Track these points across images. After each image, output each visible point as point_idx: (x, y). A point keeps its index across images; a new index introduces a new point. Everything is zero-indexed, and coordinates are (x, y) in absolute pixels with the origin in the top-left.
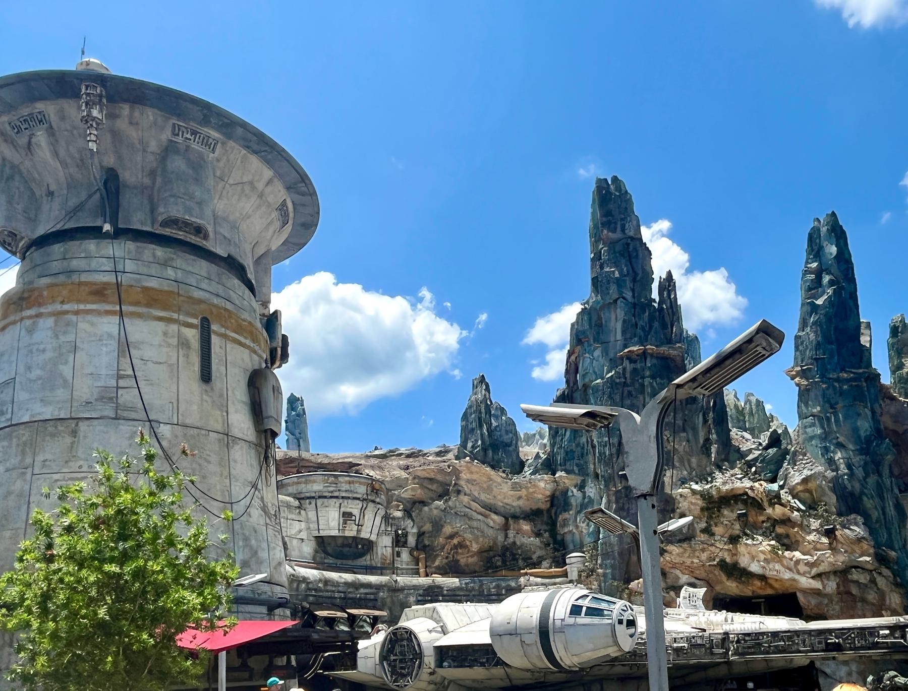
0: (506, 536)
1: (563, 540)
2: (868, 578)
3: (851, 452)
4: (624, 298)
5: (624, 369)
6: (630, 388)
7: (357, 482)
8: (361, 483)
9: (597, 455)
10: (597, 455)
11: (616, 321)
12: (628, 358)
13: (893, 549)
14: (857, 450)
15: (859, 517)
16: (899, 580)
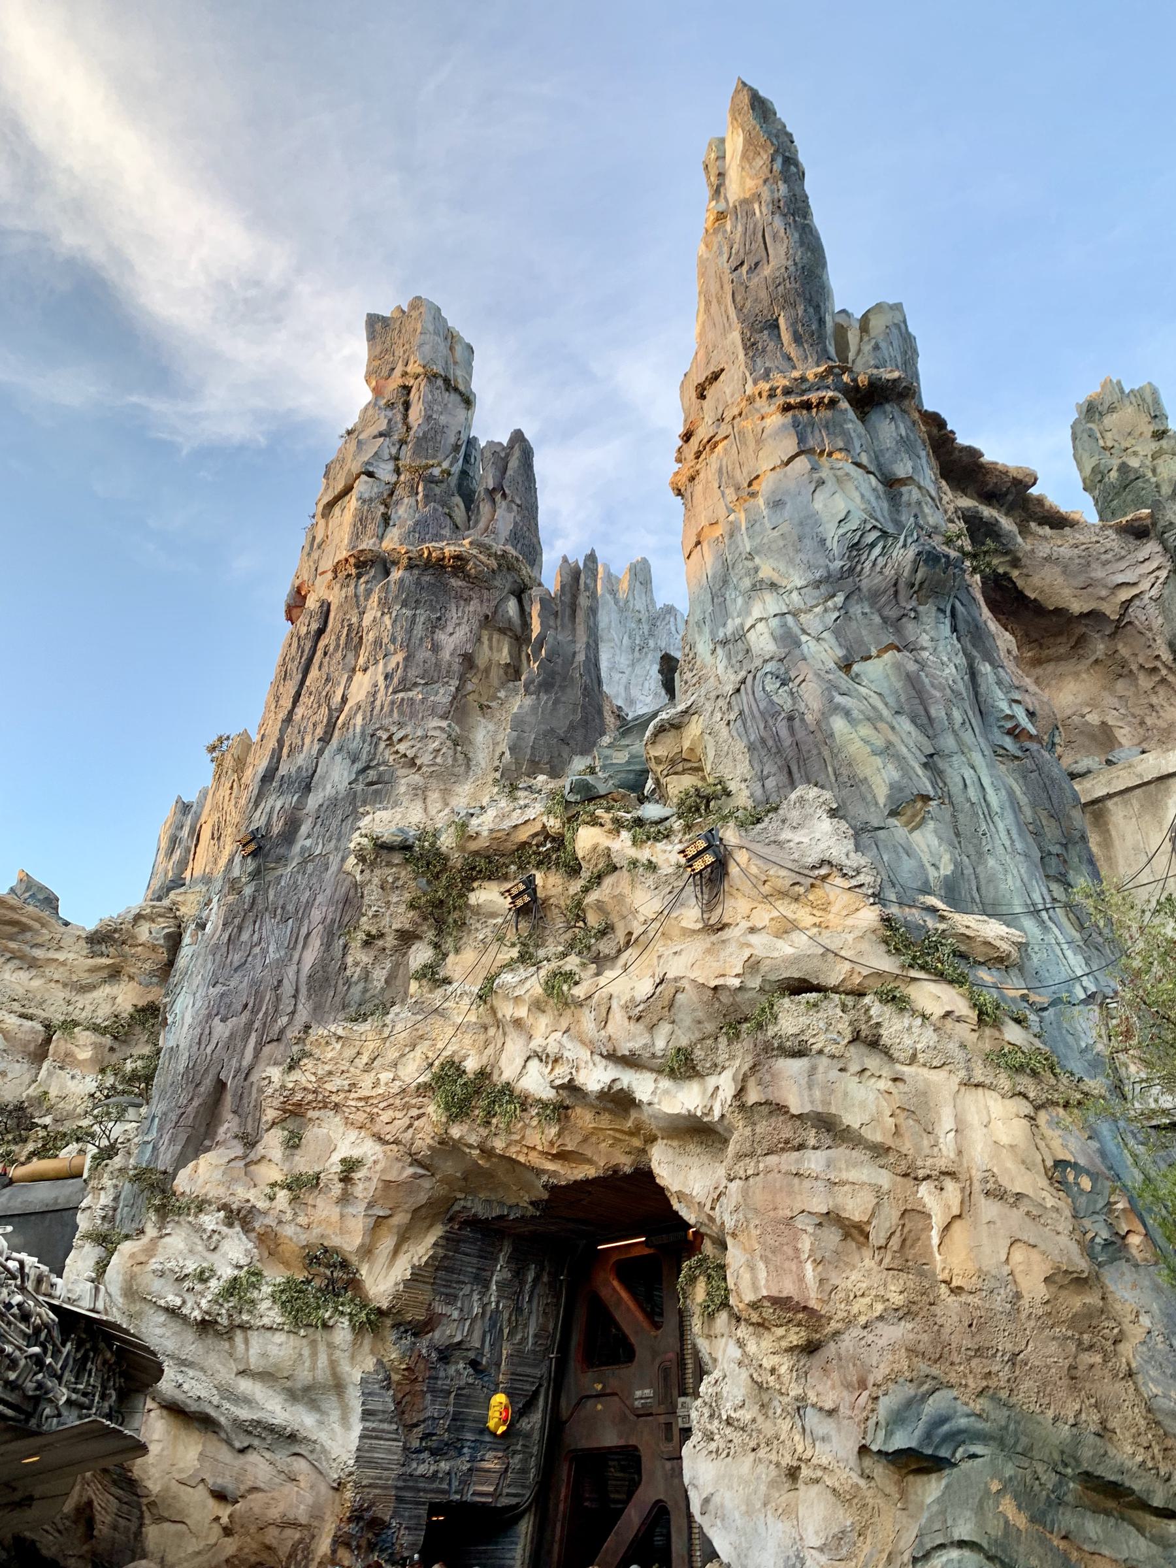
3: (795, 595)
13: (992, 910)
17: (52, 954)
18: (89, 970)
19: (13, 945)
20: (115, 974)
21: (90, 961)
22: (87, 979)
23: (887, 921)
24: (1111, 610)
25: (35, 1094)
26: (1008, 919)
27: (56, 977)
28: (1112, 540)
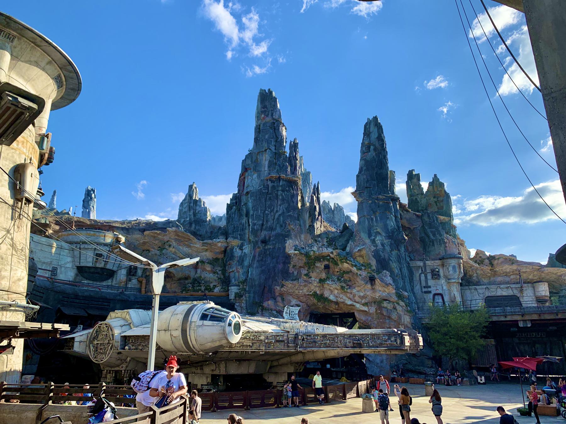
0: (196, 272)
1: (229, 276)
2: (392, 306)
4: (270, 149)
5: (268, 185)
6: (270, 196)
9: (250, 230)
10: (250, 230)
11: (265, 159)
12: (270, 180)
13: (406, 291)
14: (387, 236)
15: (388, 272)
16: (409, 309)
19: (186, 243)
20: (207, 250)
23: (396, 292)
24: (412, 228)
26: (407, 292)
28: (415, 217)
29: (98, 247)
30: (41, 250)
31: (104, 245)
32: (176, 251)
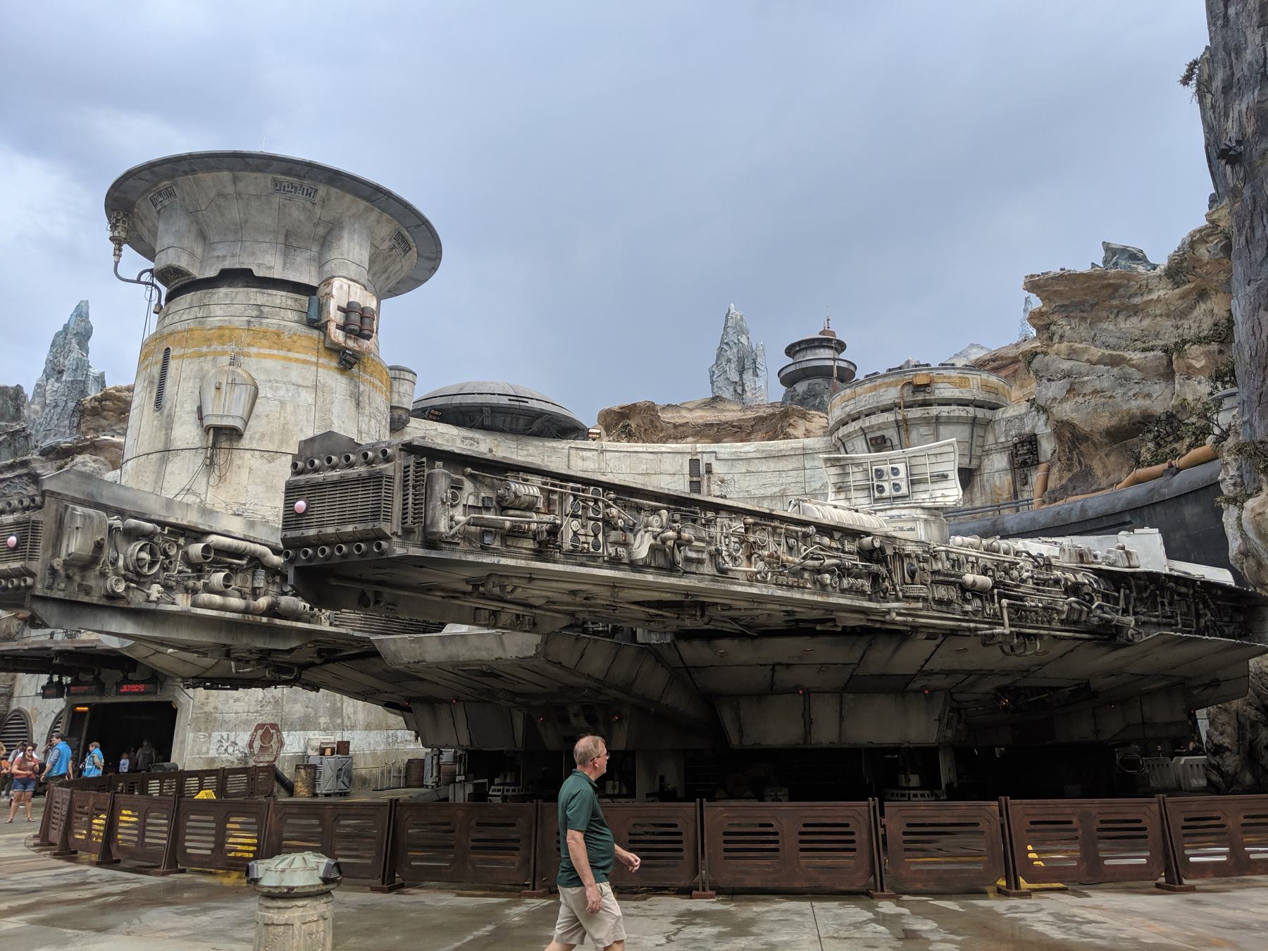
7: (880, 386)
8: (889, 385)
17: (1146, 298)
18: (1180, 298)
19: (1115, 302)
21: (1177, 290)
22: (1182, 305)
25: (1176, 403)
27: (1158, 312)
29: (866, 422)
30: (749, 472)
31: (882, 412)
32: (1077, 345)
